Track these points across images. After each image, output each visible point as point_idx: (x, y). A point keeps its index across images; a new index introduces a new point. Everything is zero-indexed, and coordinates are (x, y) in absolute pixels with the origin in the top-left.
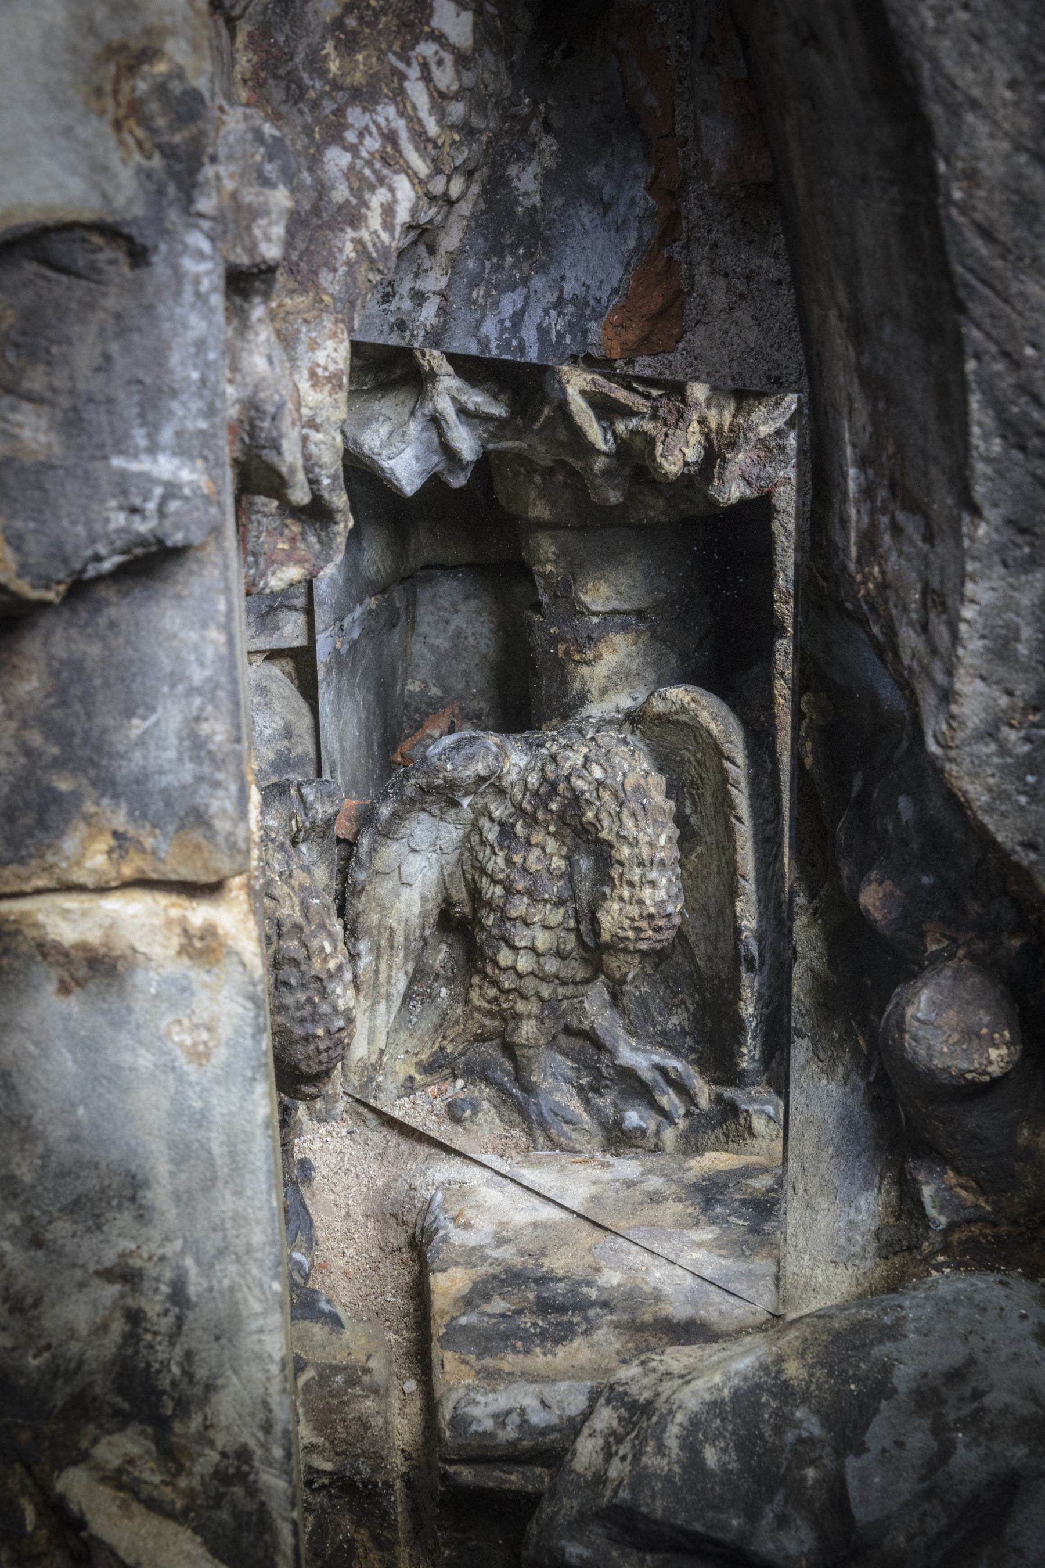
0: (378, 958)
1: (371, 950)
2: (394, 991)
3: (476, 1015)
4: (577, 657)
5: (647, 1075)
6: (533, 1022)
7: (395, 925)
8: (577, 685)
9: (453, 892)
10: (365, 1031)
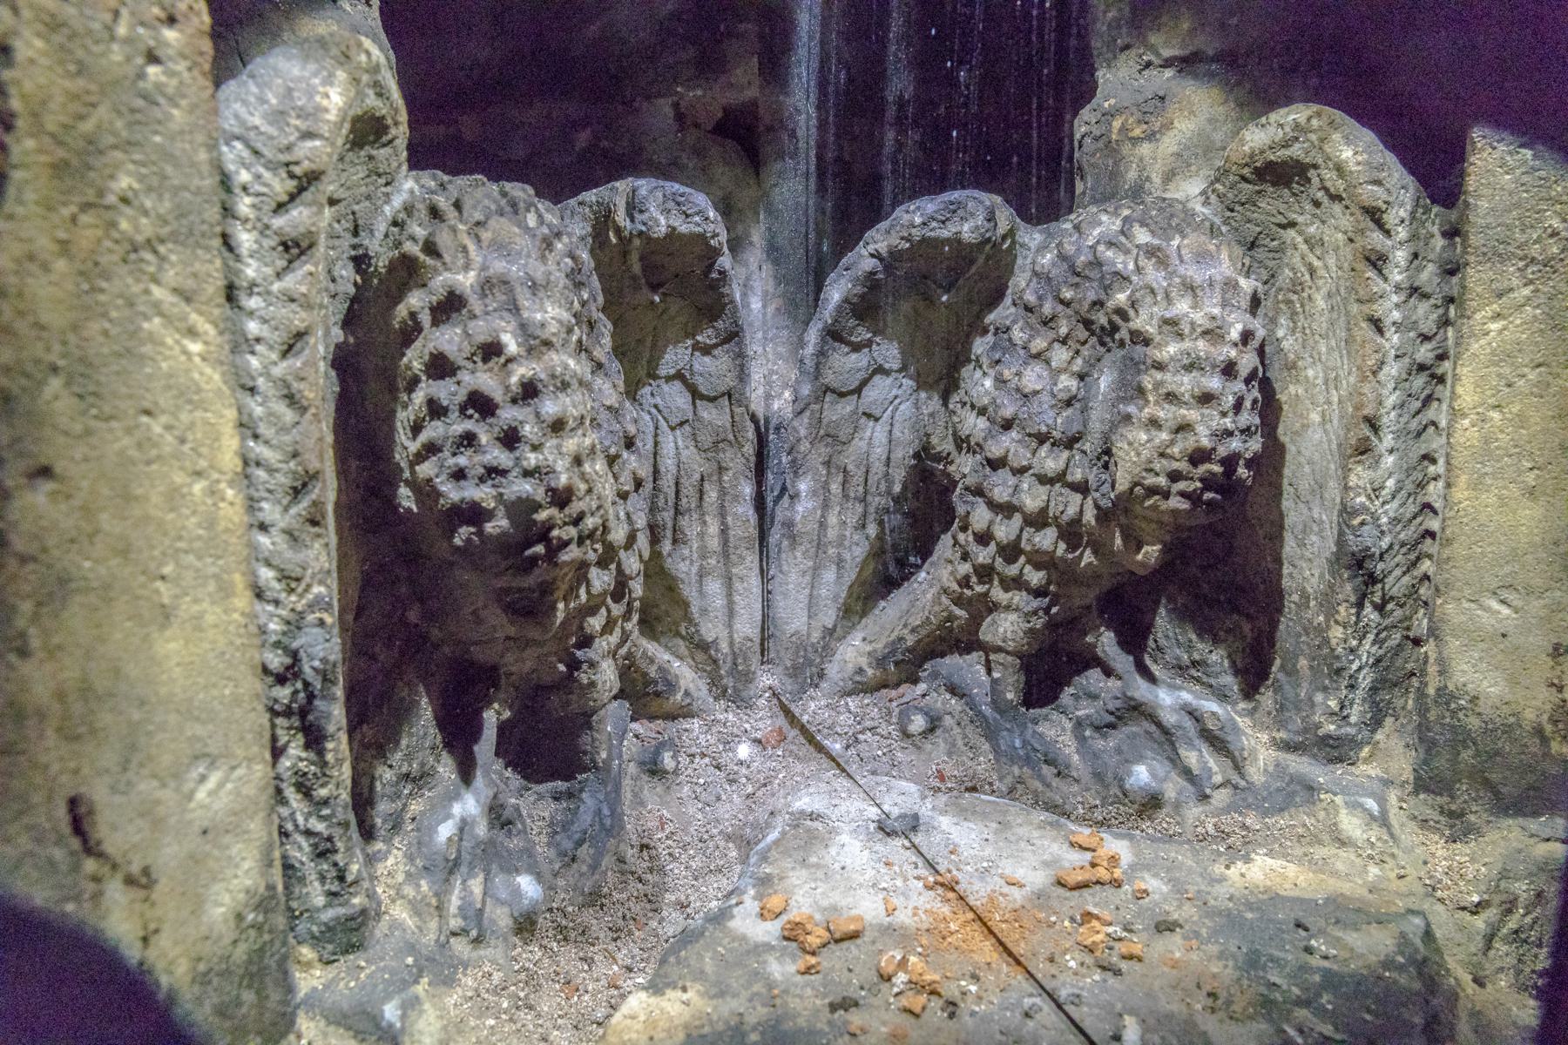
0: (826, 506)
1: (814, 493)
2: (848, 556)
3: (944, 599)
4: (1137, 132)
5: (1170, 718)
6: (1013, 617)
7: (850, 467)
8: (1132, 175)
9: (934, 440)
10: (803, 596)
